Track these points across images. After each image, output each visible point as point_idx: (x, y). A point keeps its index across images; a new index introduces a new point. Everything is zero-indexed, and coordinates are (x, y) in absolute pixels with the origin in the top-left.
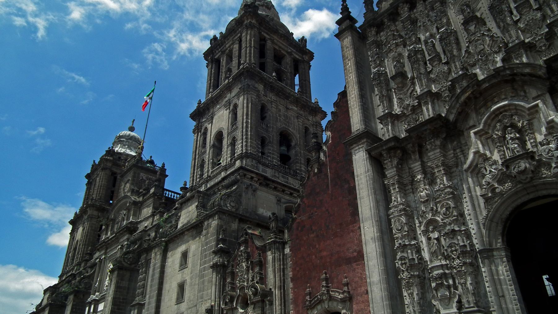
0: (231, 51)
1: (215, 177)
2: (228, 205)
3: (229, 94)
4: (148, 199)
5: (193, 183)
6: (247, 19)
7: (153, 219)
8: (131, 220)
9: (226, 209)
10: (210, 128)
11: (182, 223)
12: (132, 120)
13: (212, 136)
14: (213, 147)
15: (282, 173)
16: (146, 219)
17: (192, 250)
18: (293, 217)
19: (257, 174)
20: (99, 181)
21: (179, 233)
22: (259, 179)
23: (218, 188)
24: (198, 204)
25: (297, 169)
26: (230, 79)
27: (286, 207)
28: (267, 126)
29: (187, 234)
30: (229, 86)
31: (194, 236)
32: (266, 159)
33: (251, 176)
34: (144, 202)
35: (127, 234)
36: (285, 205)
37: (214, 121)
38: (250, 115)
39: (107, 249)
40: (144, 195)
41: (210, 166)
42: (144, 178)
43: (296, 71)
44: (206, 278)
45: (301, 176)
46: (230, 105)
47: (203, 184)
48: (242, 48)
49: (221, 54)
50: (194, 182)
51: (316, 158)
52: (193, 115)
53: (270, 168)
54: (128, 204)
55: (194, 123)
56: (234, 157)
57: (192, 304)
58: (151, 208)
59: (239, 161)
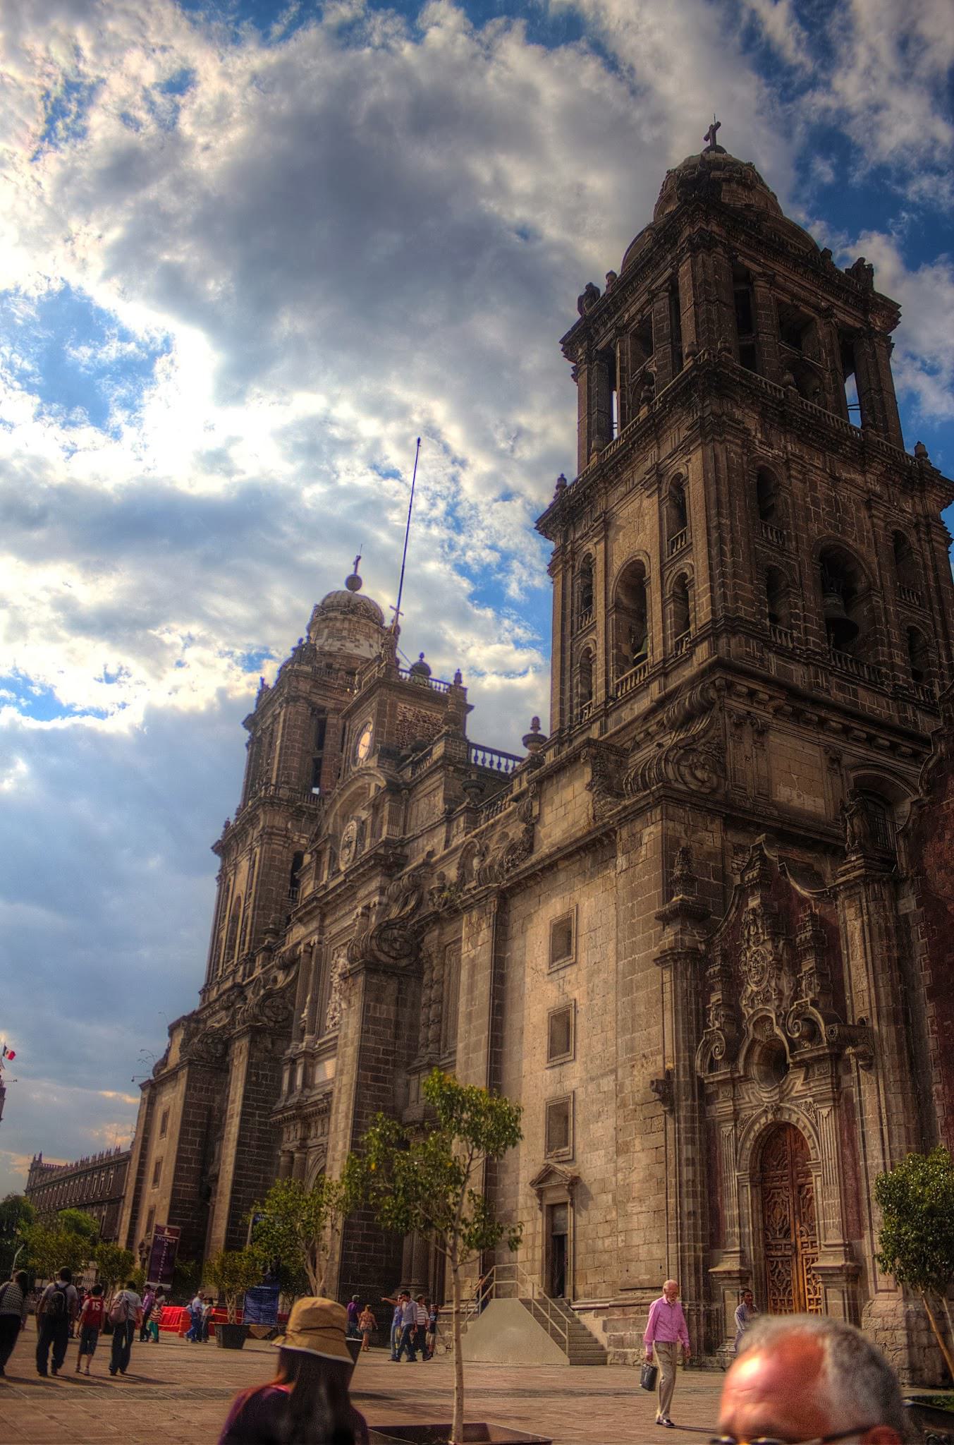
0: (646, 323)
1: (631, 698)
2: (688, 778)
3: (656, 450)
4: (430, 773)
5: (562, 722)
6: (692, 224)
7: (448, 832)
12: (354, 559)
13: (612, 581)
15: (837, 676)
17: (585, 915)
22: (771, 698)
25: (878, 663)
26: (656, 403)
27: (856, 779)
28: (779, 534)
29: (564, 869)
32: (786, 635)
33: (748, 687)
35: (377, 875)
36: (855, 774)
39: (322, 920)
42: (409, 716)
43: (849, 363)
45: (896, 685)
47: (594, 722)
48: (682, 312)
49: (616, 336)
53: (799, 661)
55: (552, 545)
56: (686, 636)
59: (705, 644)
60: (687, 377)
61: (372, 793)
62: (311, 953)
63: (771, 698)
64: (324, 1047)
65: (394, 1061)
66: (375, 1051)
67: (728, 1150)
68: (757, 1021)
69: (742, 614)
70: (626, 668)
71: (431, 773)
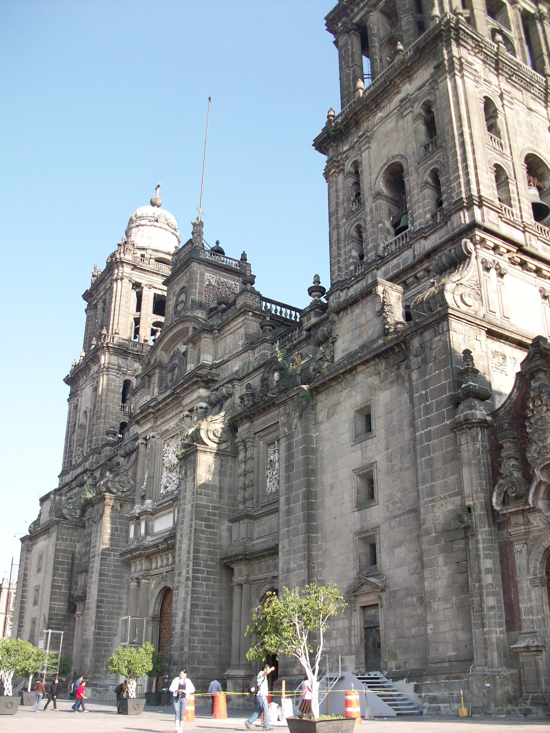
11: (343, 351)
17: (381, 403)
21: (342, 371)
29: (362, 372)
30: (407, 67)
31: (382, 374)
42: (213, 282)
44: (437, 454)
47: (367, 273)
57: (399, 509)
60: (435, 31)
61: (190, 333)
62: (146, 444)
63: (509, 251)
64: (160, 507)
65: (220, 513)
66: (207, 507)
67: (520, 560)
68: (543, 468)
70: (389, 237)
71: (236, 317)
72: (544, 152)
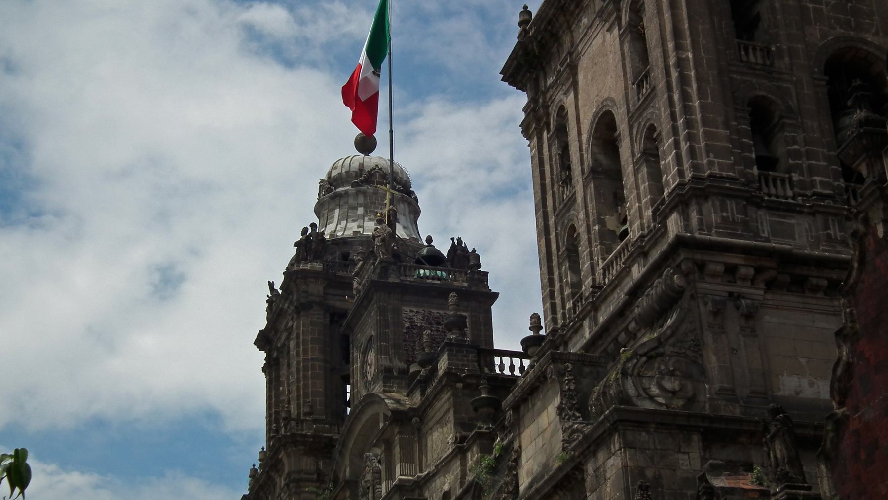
2: (655, 390)
4: (437, 395)
8: (398, 476)
9: (649, 406)
10: (573, 106)
13: (584, 137)
14: (594, 178)
16: (443, 466)
18: (835, 414)
19: (746, 251)
20: (298, 354)
22: (758, 270)
23: (626, 330)
24: (561, 403)
32: (783, 181)
34: (426, 410)
37: (581, 77)
38: (688, 33)
40: (424, 383)
41: (597, 249)
42: (418, 321)
46: (619, 10)
47: (583, 319)
50: (559, 315)
51: (874, 183)
52: (510, 71)
53: (800, 212)
54: (381, 425)
55: (523, 99)
58: (451, 425)
69: (716, 171)
72: (876, 34)
